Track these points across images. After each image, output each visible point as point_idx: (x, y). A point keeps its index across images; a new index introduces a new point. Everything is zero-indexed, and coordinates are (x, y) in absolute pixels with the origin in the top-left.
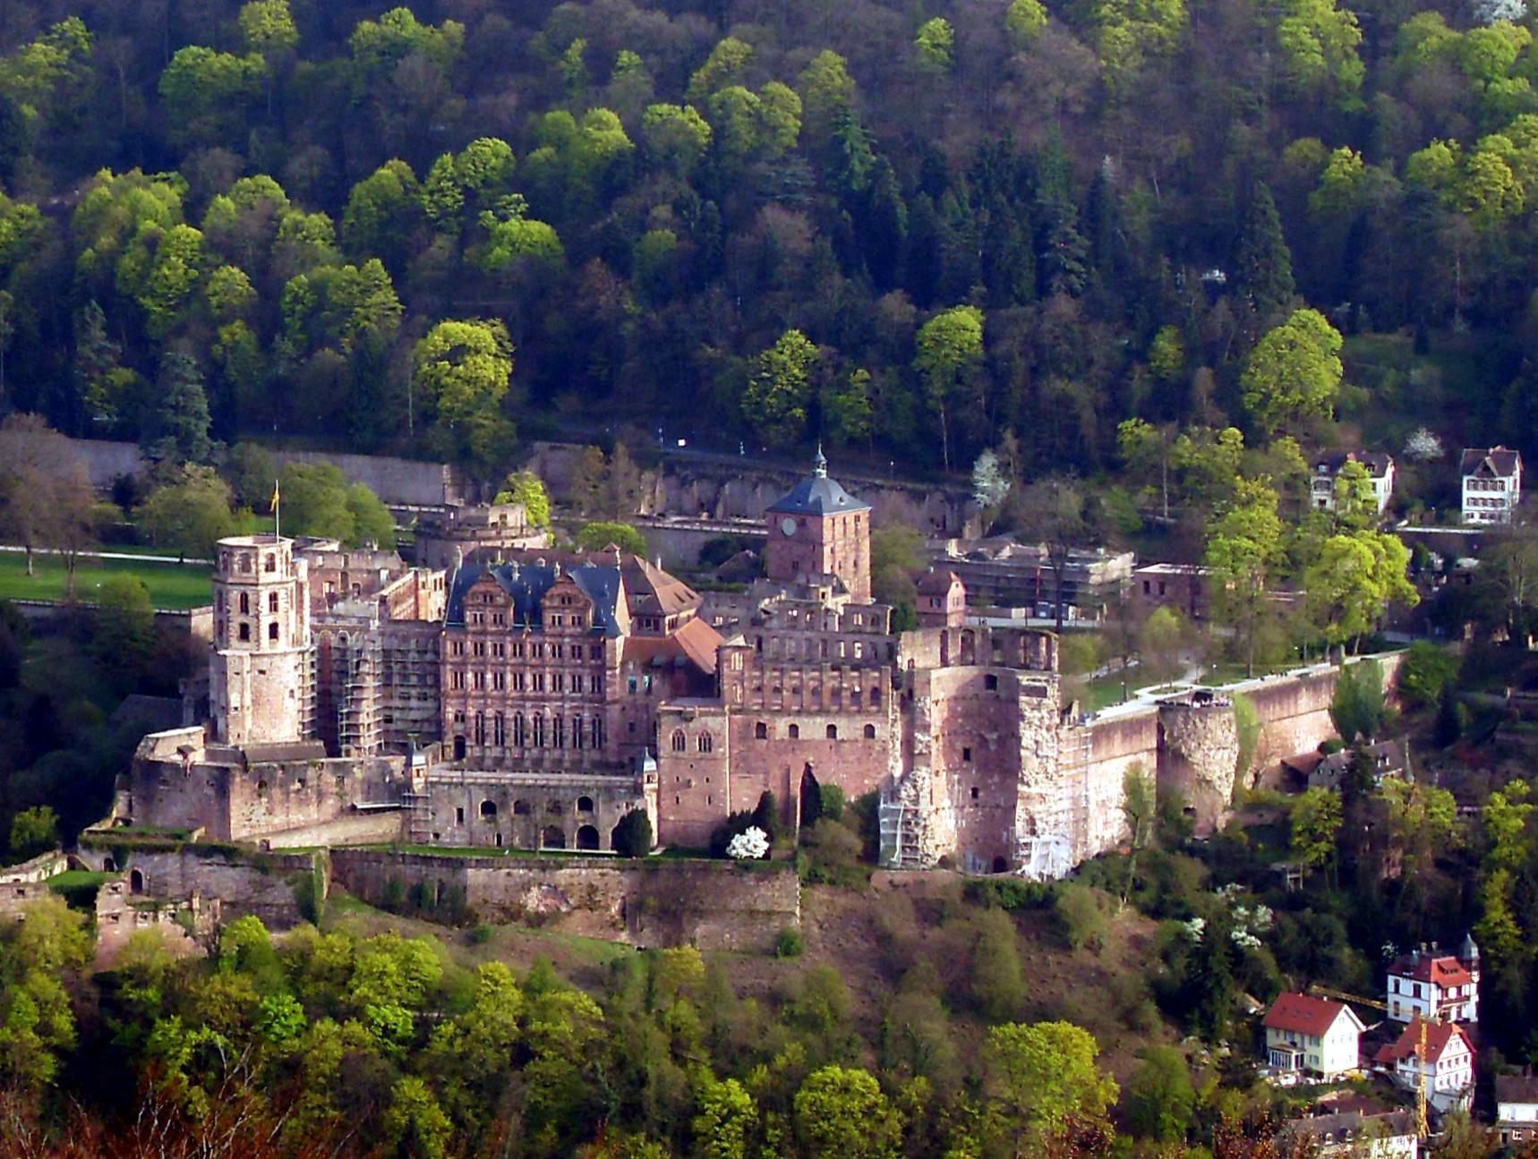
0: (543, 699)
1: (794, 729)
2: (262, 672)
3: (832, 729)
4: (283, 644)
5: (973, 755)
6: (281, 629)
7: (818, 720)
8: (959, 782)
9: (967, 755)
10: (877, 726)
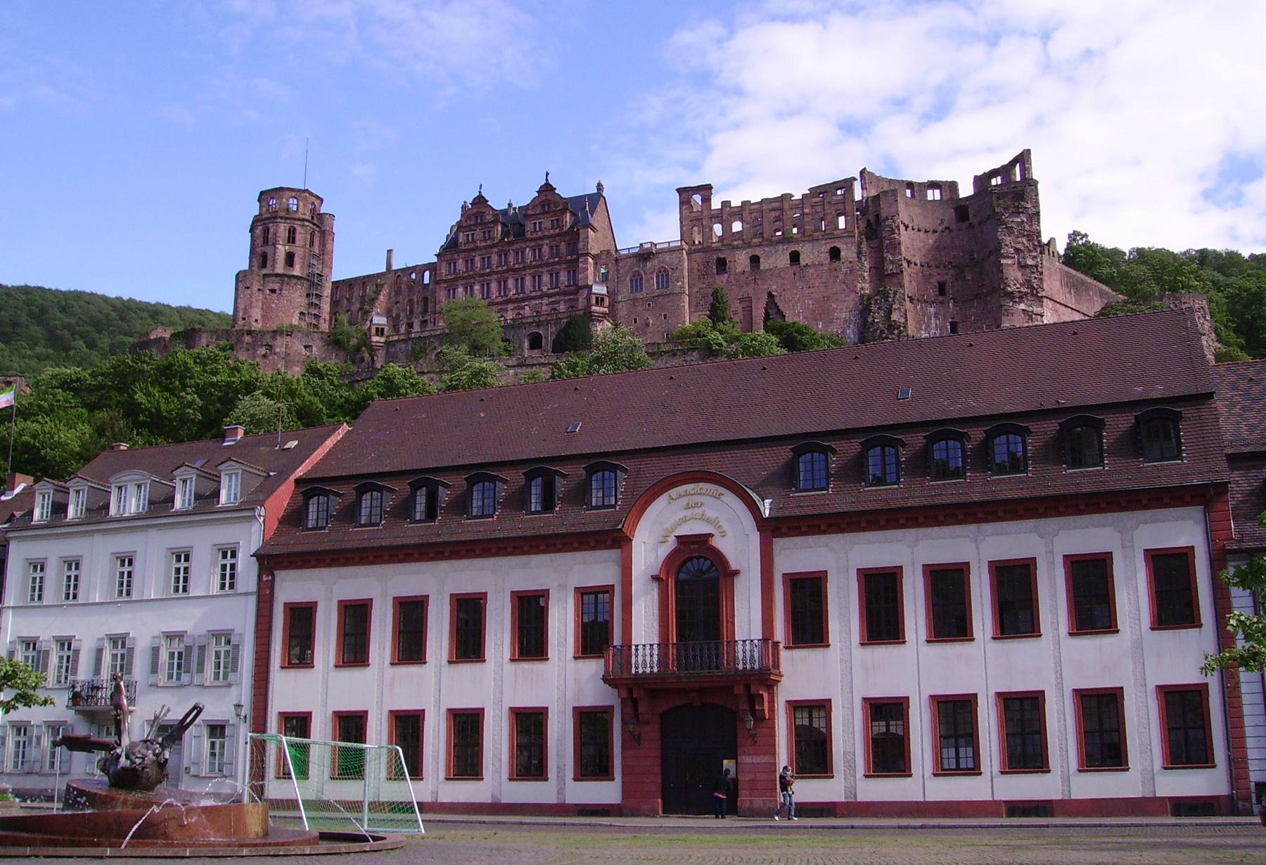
0: (524, 300)
1: (755, 260)
2: (273, 291)
3: (795, 257)
4: (297, 271)
5: (950, 291)
6: (297, 260)
7: (780, 247)
8: (936, 315)
9: (942, 289)
10: (837, 245)
